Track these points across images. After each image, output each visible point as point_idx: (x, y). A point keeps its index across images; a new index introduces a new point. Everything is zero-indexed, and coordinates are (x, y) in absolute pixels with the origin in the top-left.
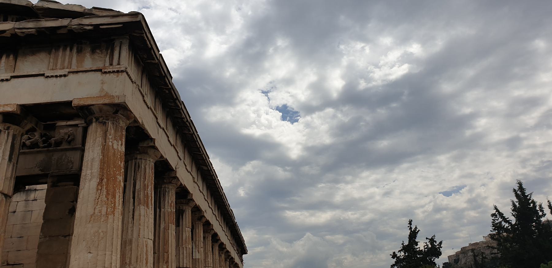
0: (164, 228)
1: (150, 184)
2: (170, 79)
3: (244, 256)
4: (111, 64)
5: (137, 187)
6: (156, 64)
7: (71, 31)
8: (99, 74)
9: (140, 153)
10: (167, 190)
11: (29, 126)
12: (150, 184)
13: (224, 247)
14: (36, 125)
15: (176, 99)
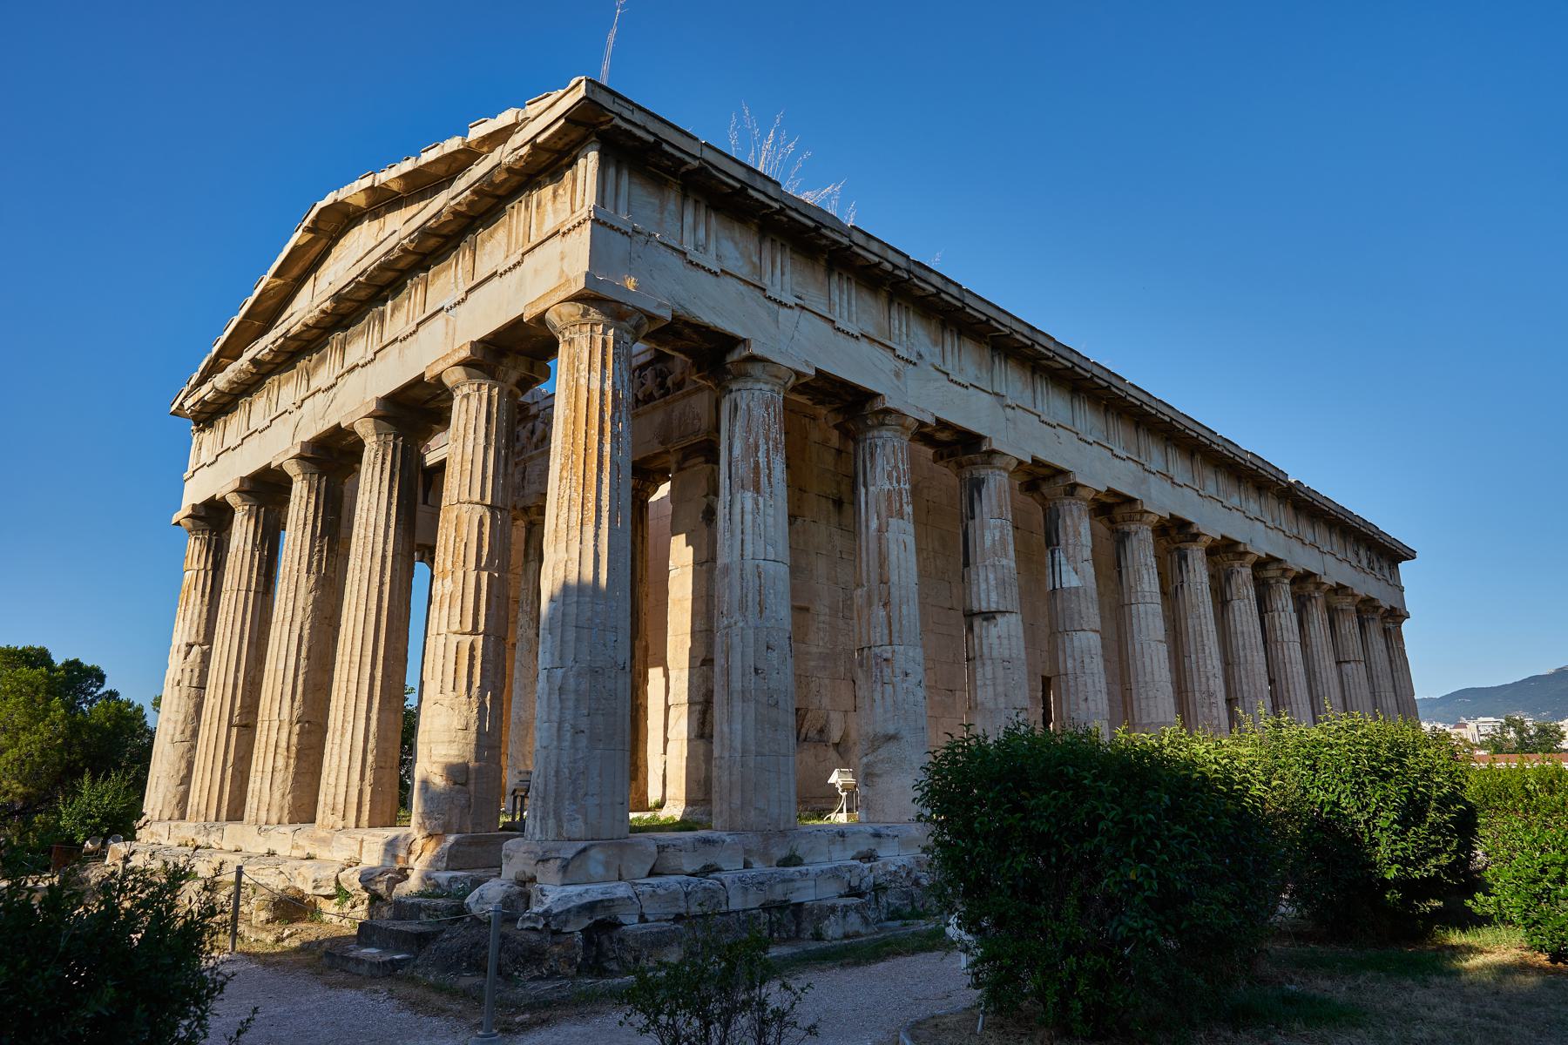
0: (879, 530)
1: (762, 441)
2: (771, 190)
3: (1403, 566)
4: (573, 212)
5: (737, 452)
6: (701, 170)
7: (509, 170)
8: (559, 237)
9: (735, 378)
10: (879, 442)
11: (514, 376)
12: (762, 441)
13: (1241, 548)
14: (531, 370)
15: (817, 229)
